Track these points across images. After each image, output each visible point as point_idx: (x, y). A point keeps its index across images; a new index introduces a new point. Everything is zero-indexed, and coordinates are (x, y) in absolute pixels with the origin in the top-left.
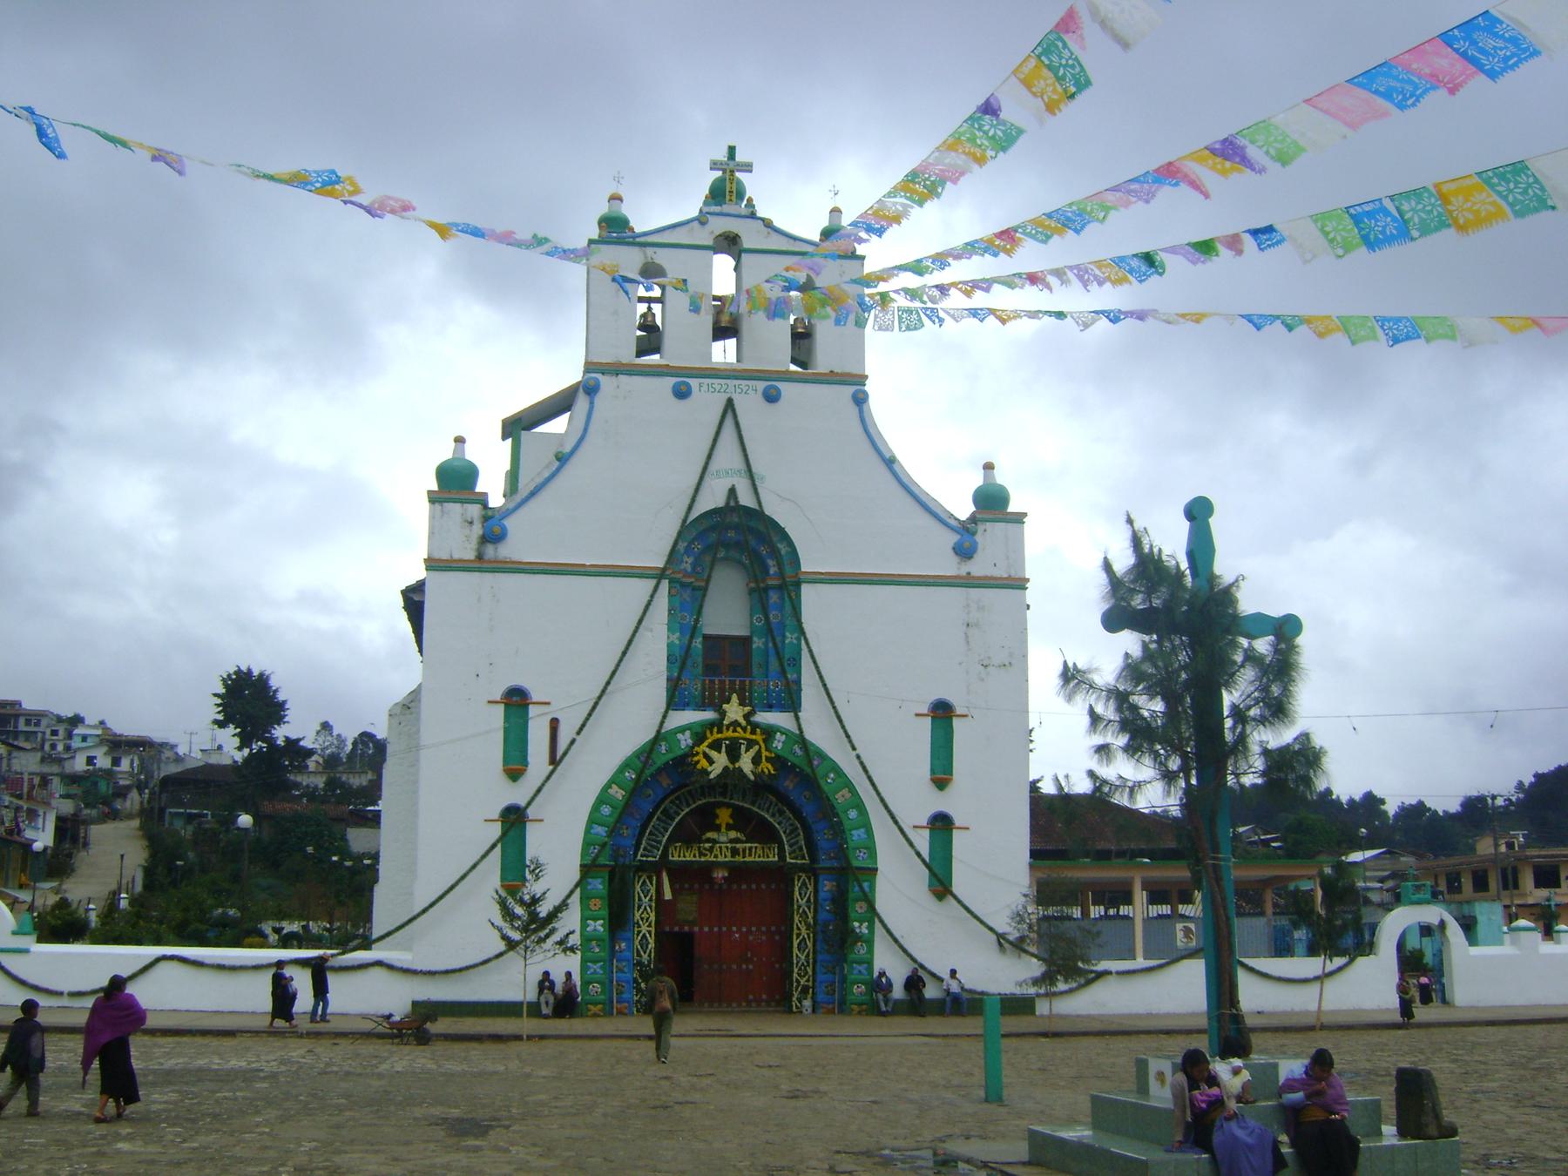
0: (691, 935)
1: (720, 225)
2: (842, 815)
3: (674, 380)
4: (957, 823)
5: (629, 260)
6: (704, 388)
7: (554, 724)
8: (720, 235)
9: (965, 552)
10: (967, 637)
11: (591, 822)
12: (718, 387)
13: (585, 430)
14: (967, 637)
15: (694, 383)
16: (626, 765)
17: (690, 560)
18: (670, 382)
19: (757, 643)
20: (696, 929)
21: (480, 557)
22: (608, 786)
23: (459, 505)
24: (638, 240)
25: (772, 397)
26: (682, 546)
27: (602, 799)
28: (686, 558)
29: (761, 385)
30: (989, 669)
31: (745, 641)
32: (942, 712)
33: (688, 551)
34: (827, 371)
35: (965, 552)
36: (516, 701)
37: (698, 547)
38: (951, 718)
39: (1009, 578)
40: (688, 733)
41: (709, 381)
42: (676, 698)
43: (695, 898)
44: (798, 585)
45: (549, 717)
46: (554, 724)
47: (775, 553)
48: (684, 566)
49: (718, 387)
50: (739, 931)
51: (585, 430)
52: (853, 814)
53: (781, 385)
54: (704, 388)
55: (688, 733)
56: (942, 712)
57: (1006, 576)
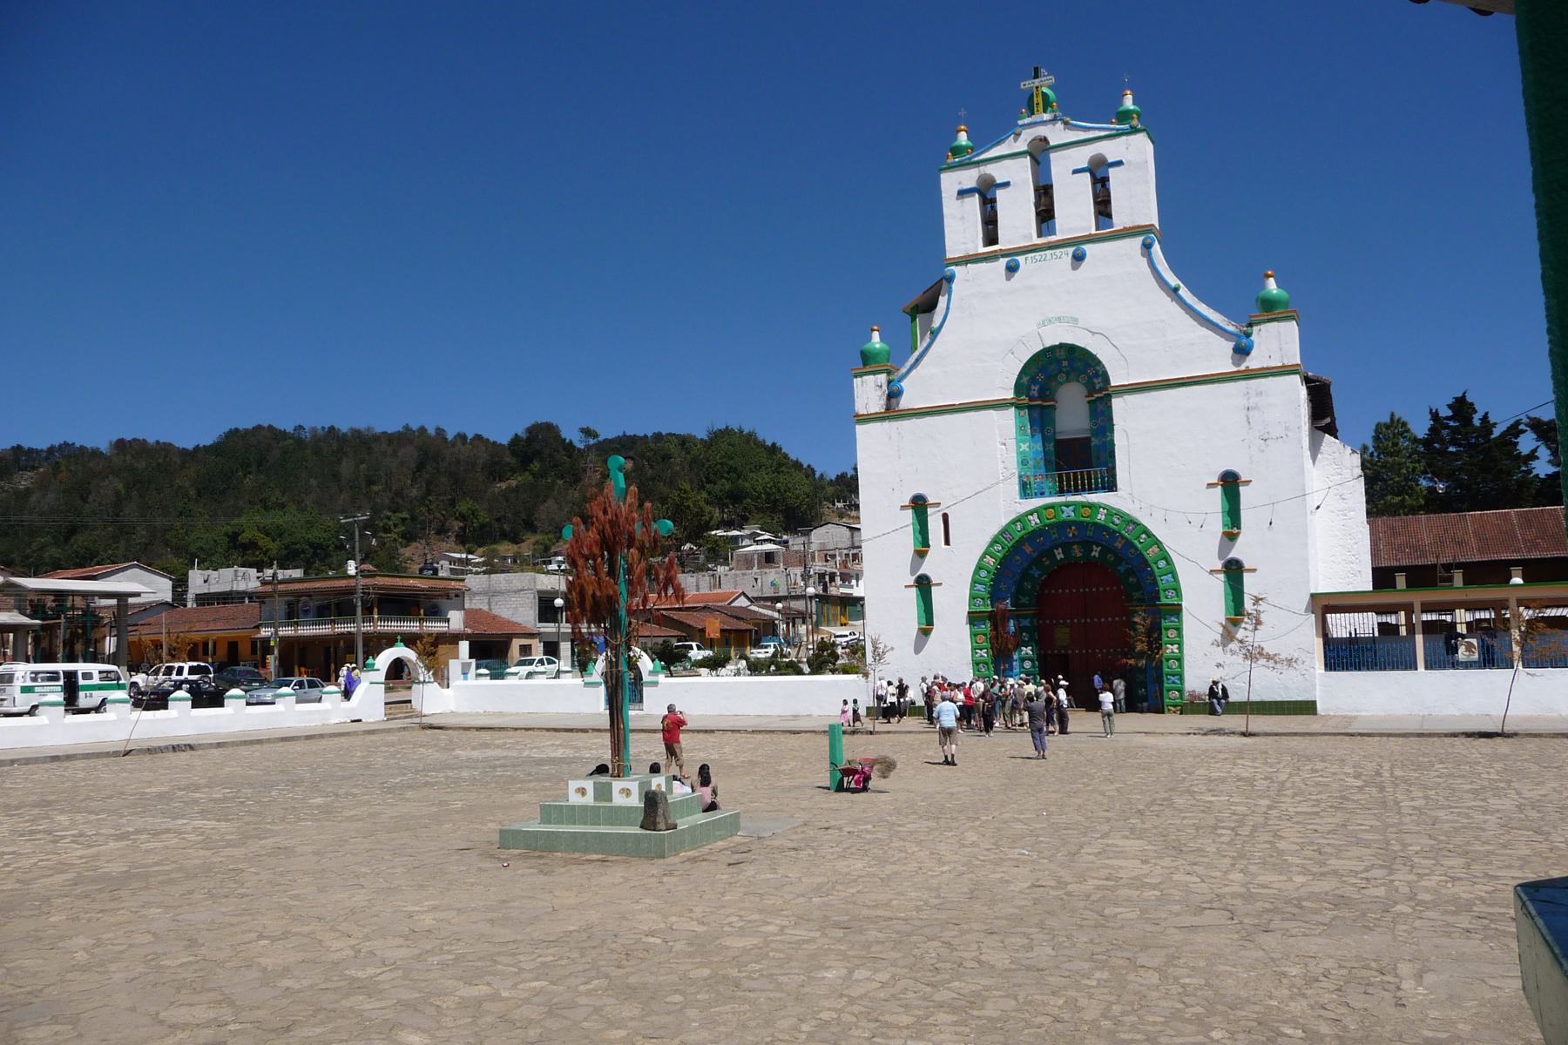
0: (1066, 656)
1: (1027, 136)
2: (1154, 567)
3: (1007, 259)
4: (1247, 566)
5: (969, 178)
6: (1030, 260)
7: (945, 518)
8: (1033, 140)
9: (1242, 351)
10: (1248, 418)
11: (974, 582)
12: (1039, 258)
13: (948, 308)
14: (1248, 418)
15: (1021, 259)
16: (995, 541)
17: (1037, 388)
18: (1003, 262)
19: (1095, 441)
20: (1070, 652)
21: (888, 409)
22: (983, 557)
23: (871, 377)
24: (976, 159)
25: (1078, 258)
26: (1025, 379)
27: (979, 568)
28: (1033, 387)
29: (1071, 250)
30: (1268, 442)
31: (1088, 440)
32: (1230, 483)
33: (1033, 381)
34: (1121, 228)
35: (1242, 351)
36: (919, 505)
37: (1041, 378)
38: (1237, 486)
39: (1283, 366)
40: (1035, 515)
41: (1033, 255)
42: (1026, 490)
43: (1067, 630)
44: (1108, 397)
45: (941, 513)
46: (945, 518)
47: (1097, 372)
48: (1100, 380)
49: (1039, 258)
50: (1101, 652)
51: (948, 308)
52: (1162, 564)
53: (1086, 247)
54: (1030, 260)
55: (1035, 515)
56: (1230, 483)
57: (1280, 364)
